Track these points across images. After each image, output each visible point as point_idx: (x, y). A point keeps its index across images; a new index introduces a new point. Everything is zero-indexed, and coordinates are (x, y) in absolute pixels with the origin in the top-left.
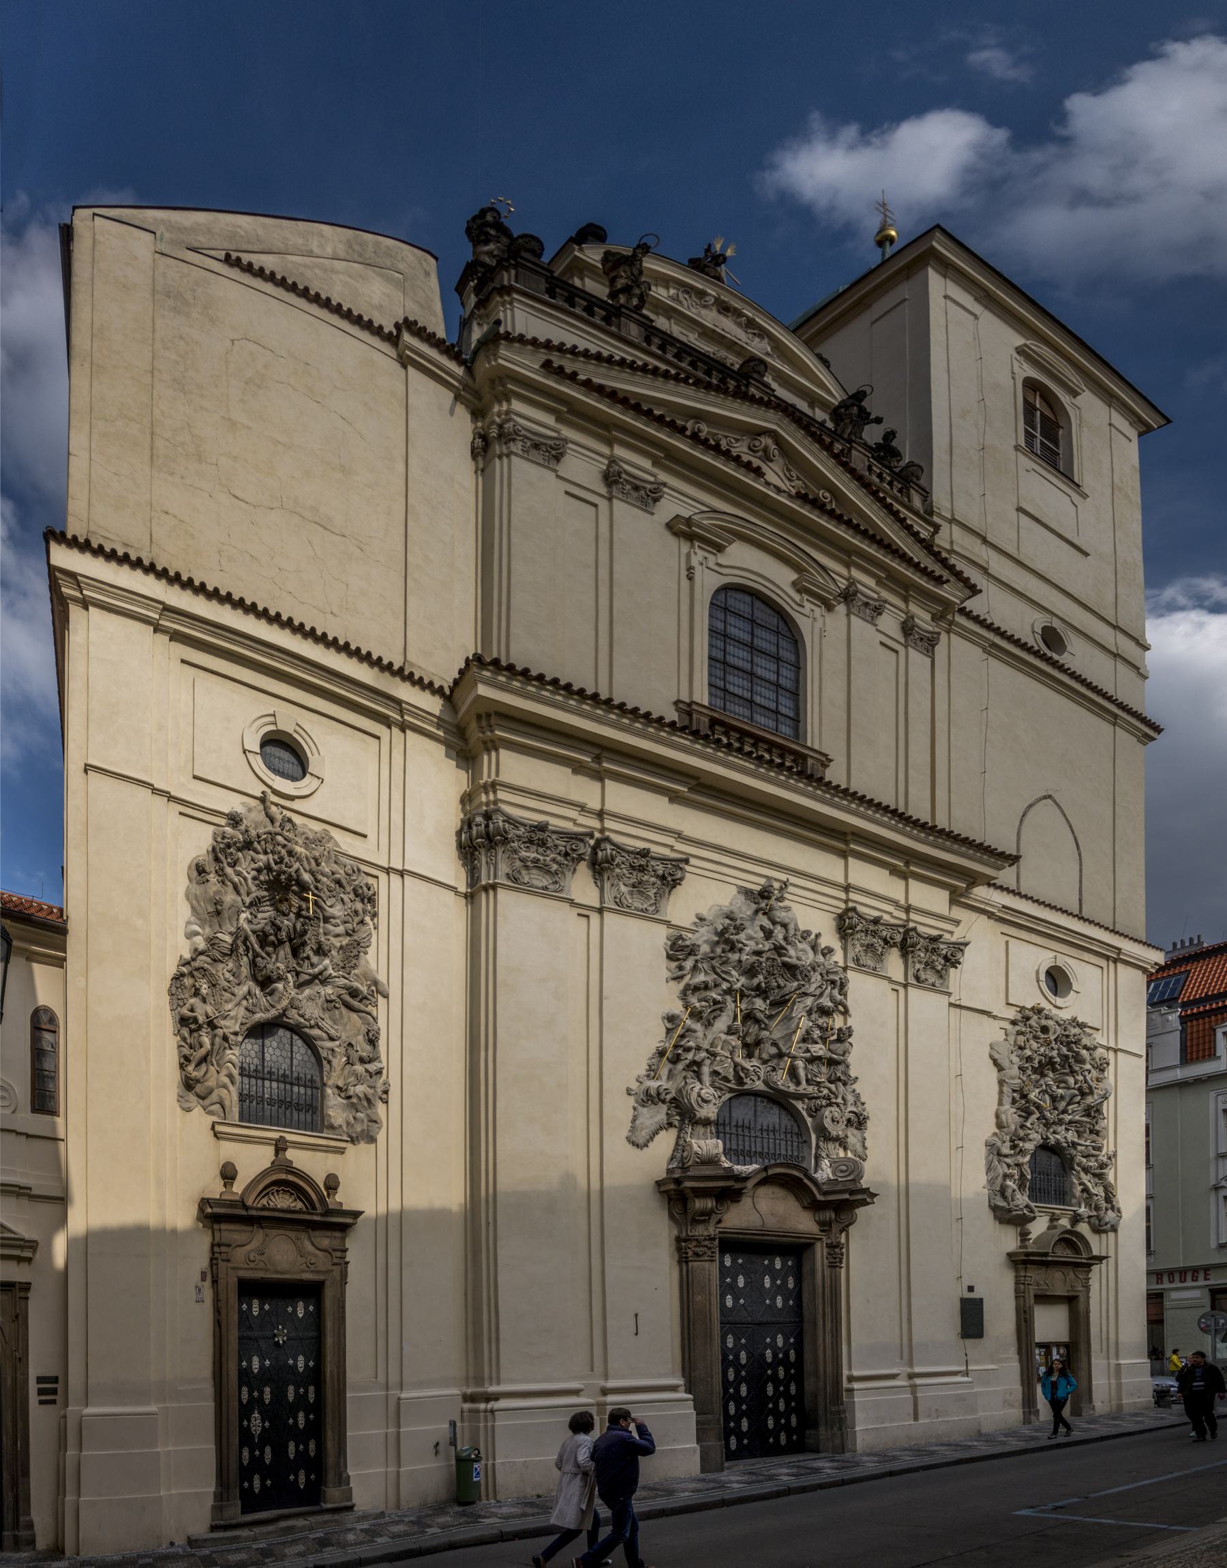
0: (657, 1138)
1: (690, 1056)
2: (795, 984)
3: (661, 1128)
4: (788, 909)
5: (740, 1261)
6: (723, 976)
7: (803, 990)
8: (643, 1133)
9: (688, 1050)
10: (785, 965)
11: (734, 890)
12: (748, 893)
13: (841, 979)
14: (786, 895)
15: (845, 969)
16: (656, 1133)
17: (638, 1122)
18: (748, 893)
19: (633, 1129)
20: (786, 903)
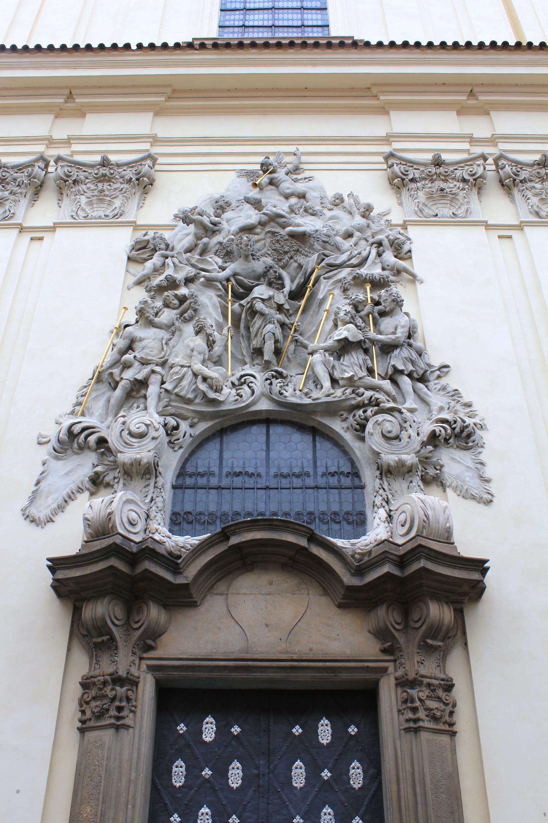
0: (72, 505)
1: (129, 375)
2: (315, 256)
3: (80, 490)
4: (310, 179)
5: (236, 730)
6: (201, 266)
7: (327, 261)
8: (50, 501)
9: (127, 366)
10: (293, 236)
11: (233, 175)
12: (249, 175)
13: (387, 237)
14: (302, 166)
15: (404, 226)
16: (70, 497)
17: (43, 484)
18: (249, 175)
19: (34, 498)
20: (307, 174)
